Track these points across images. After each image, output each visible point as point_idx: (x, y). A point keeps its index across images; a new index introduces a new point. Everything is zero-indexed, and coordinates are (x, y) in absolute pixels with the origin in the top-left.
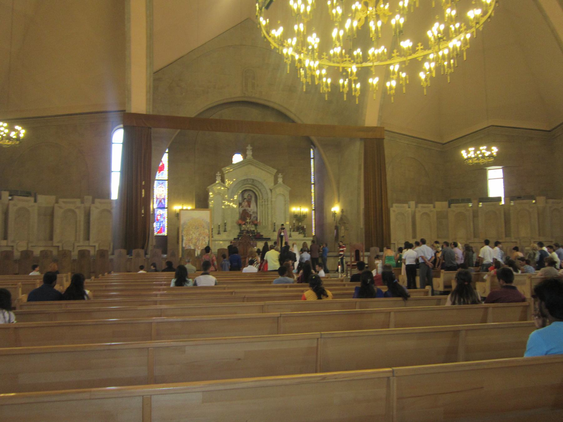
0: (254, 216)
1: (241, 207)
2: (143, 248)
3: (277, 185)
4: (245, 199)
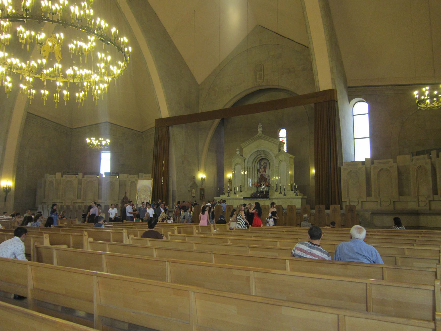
0: (268, 179)
1: (259, 172)
2: (339, 204)
3: (280, 152)
4: (262, 166)
